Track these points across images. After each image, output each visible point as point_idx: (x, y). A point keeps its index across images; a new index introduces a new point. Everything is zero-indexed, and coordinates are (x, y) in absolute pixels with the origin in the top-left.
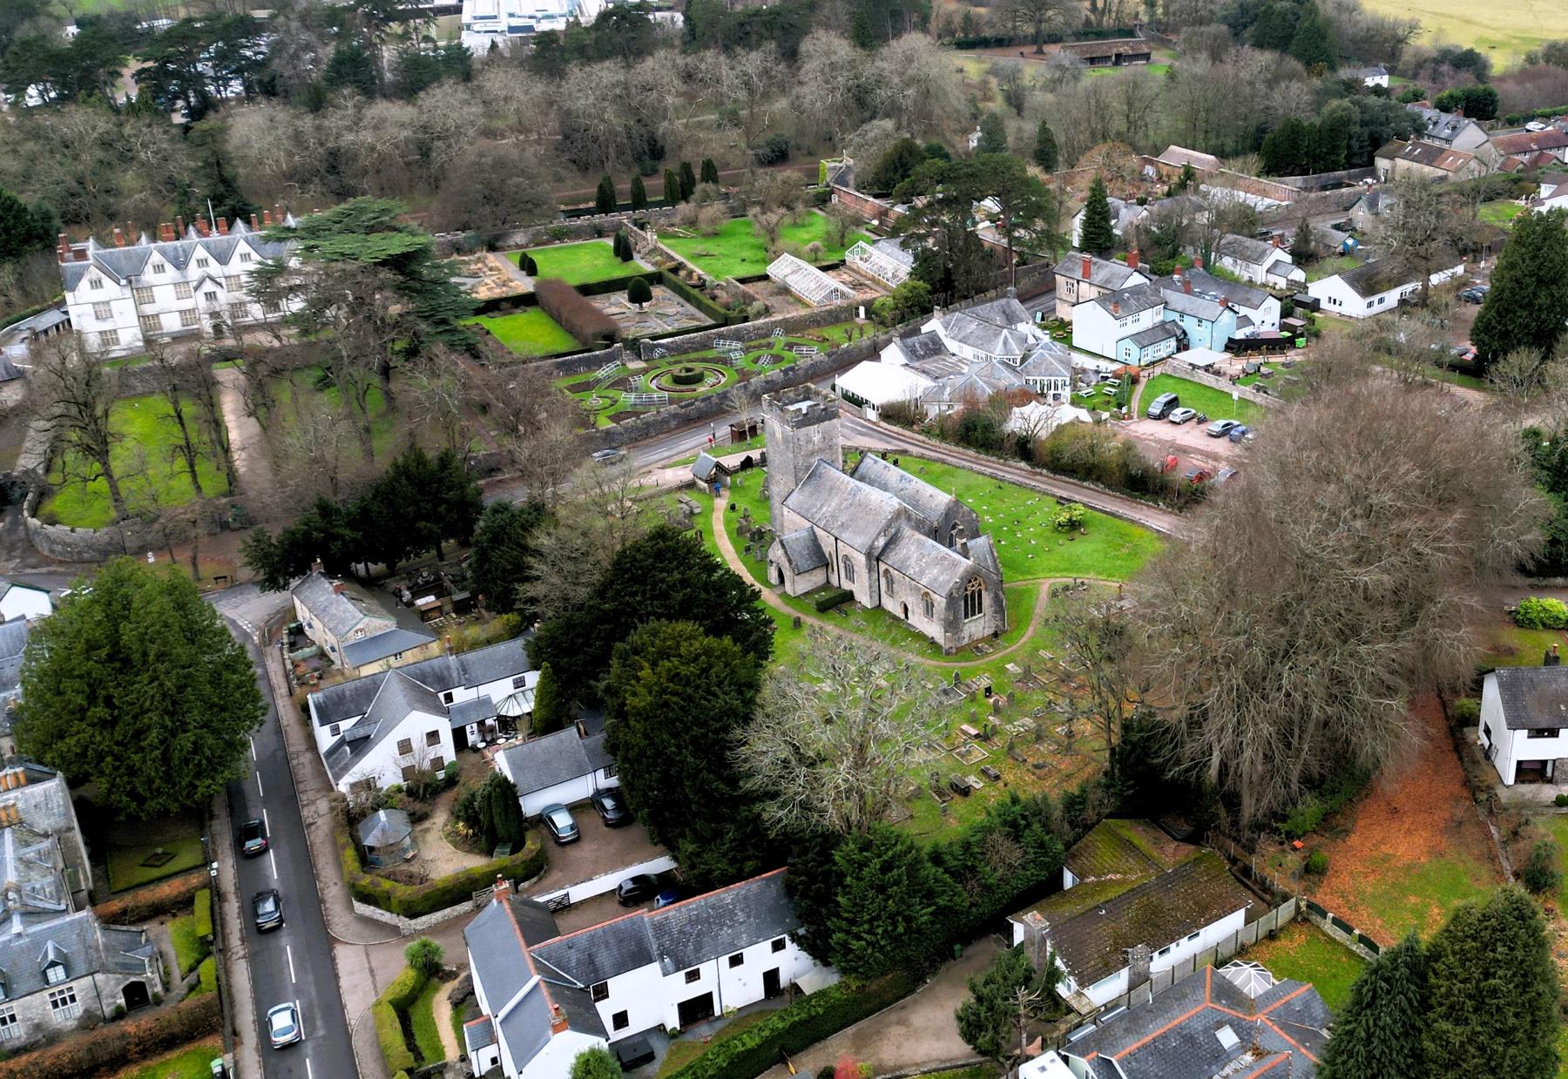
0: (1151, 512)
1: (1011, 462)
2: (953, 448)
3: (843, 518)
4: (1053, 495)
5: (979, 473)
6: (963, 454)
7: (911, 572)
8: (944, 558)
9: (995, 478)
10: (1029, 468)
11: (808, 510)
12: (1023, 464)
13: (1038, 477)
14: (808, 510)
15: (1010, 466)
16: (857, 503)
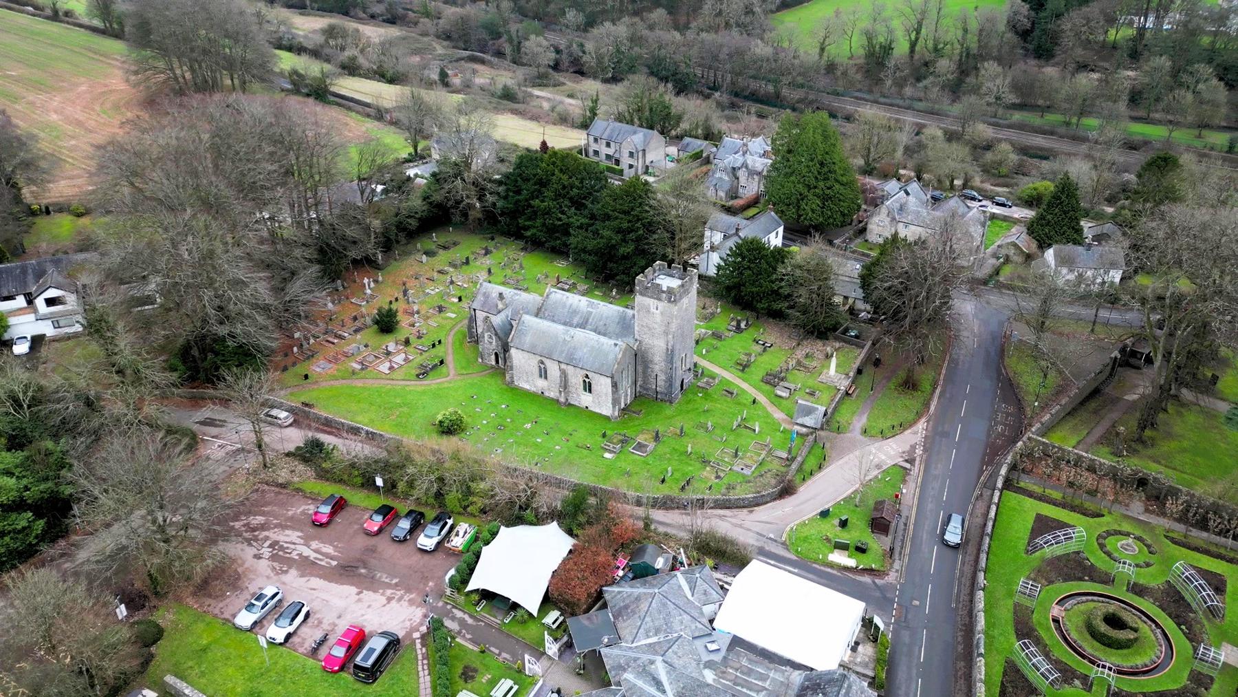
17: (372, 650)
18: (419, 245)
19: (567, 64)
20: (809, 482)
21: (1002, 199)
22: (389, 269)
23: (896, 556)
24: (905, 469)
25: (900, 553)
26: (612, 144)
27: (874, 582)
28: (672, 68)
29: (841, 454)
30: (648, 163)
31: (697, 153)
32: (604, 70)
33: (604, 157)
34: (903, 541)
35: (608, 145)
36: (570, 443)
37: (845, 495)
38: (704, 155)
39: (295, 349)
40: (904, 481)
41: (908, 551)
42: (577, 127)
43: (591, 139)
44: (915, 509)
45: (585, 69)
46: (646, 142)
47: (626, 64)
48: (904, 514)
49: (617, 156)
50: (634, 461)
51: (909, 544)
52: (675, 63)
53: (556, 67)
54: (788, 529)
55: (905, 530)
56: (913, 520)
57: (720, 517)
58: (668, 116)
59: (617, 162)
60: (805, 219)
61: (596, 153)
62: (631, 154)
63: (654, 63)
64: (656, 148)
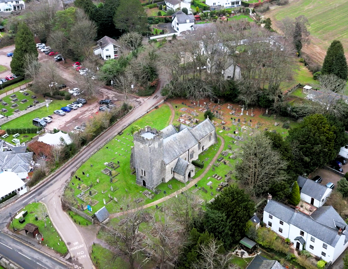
0: (120, 123)
1: (81, 150)
2: (64, 165)
3: (183, 145)
4: (115, 136)
5: (94, 154)
6: (68, 163)
7: (204, 135)
8: (203, 125)
9: (100, 149)
10: (86, 146)
11: (174, 156)
12: (84, 147)
13: (92, 145)
14: (174, 156)
15: (81, 152)
16: (179, 140)
17: (37, 120)
18: (289, 122)
20: (68, 216)
22: (265, 117)
23: (14, 234)
24: (65, 256)
25: (15, 236)
27: (6, 223)
29: (84, 233)
34: (22, 239)
36: (118, 155)
37: (54, 224)
39: (195, 104)
40: (57, 252)
41: (15, 239)
44: (38, 250)
48: (37, 245)
50: (100, 169)
51: (19, 241)
54: (44, 204)
55: (27, 242)
56: (30, 246)
57: (60, 189)
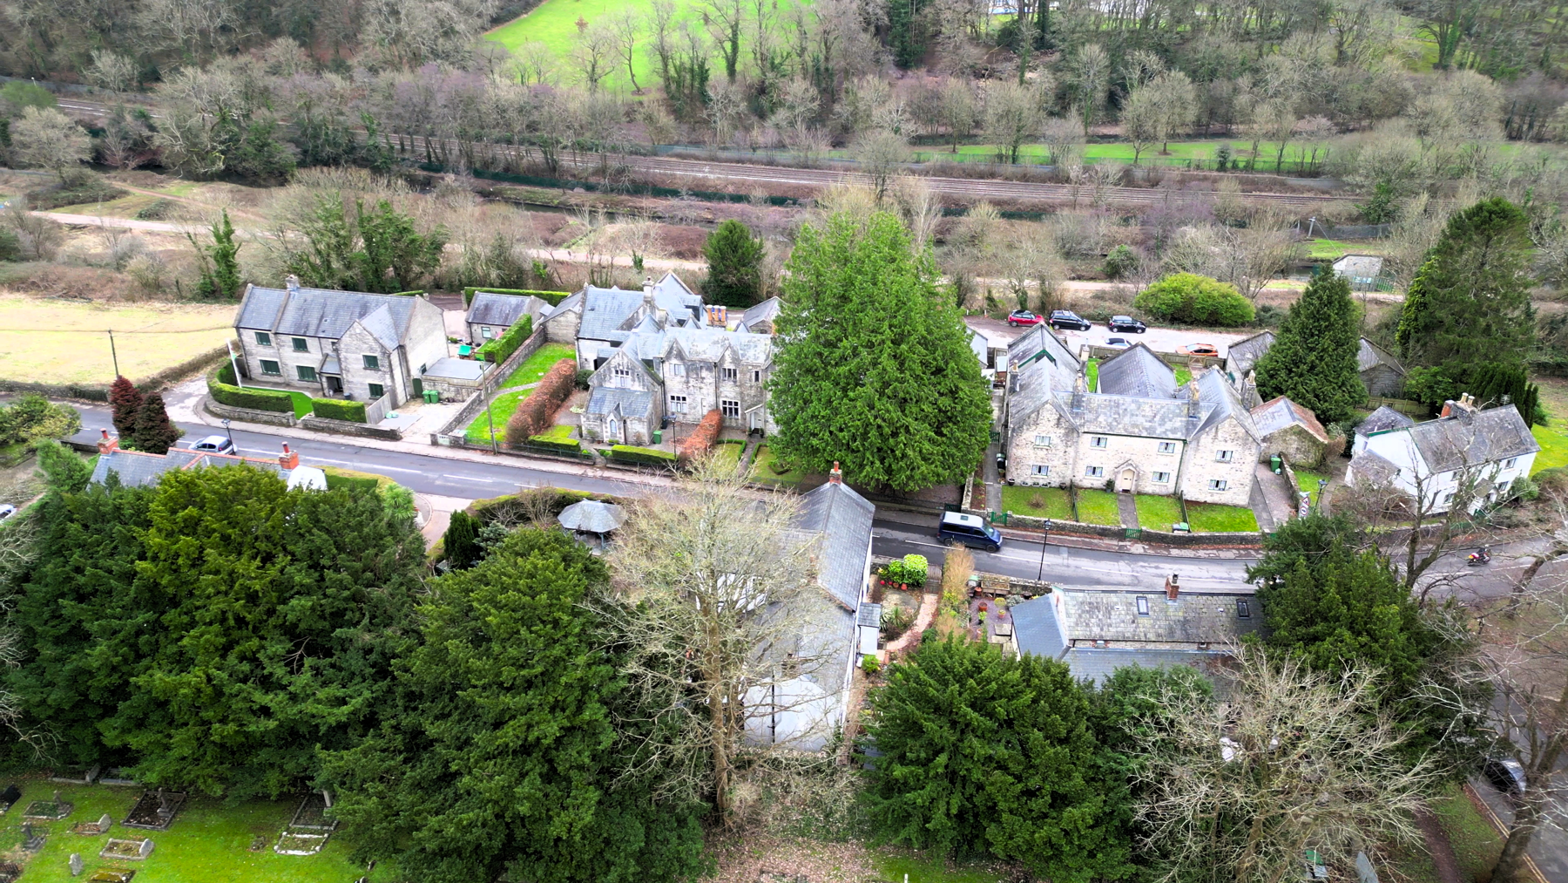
19: (121, 154)
21: (1127, 320)
26: (309, 341)
28: (343, 140)
30: (416, 373)
31: (522, 328)
32: (203, 156)
33: (295, 375)
35: (300, 345)
38: (534, 327)
42: (194, 299)
43: (249, 338)
45: (163, 159)
46: (401, 327)
47: (249, 142)
49: (331, 368)
52: (346, 130)
53: (99, 161)
58: (413, 248)
59: (336, 385)
60: (910, 478)
61: (270, 367)
62: (371, 362)
63: (304, 134)
64: (426, 335)
